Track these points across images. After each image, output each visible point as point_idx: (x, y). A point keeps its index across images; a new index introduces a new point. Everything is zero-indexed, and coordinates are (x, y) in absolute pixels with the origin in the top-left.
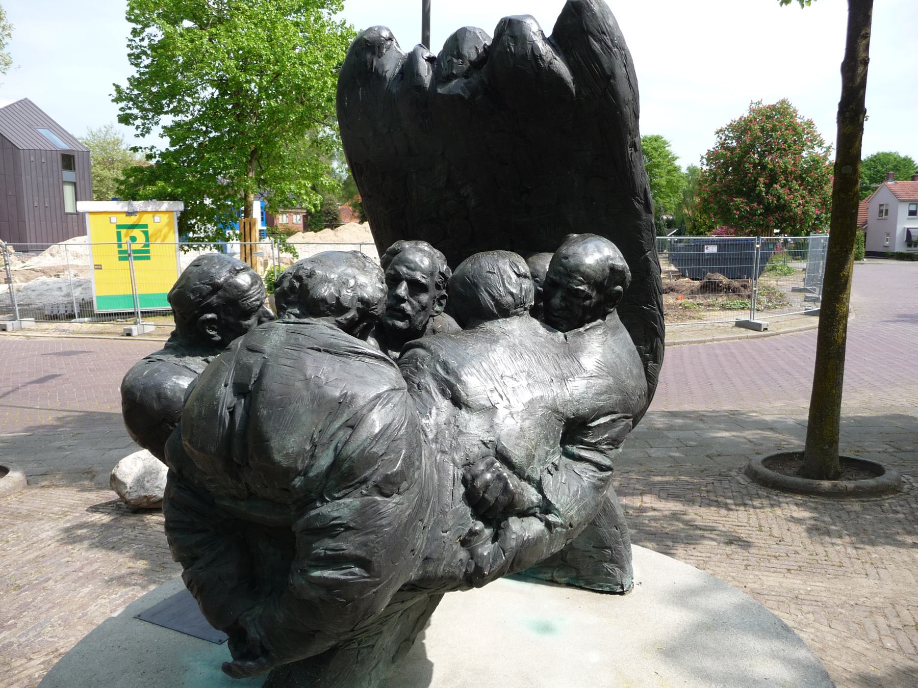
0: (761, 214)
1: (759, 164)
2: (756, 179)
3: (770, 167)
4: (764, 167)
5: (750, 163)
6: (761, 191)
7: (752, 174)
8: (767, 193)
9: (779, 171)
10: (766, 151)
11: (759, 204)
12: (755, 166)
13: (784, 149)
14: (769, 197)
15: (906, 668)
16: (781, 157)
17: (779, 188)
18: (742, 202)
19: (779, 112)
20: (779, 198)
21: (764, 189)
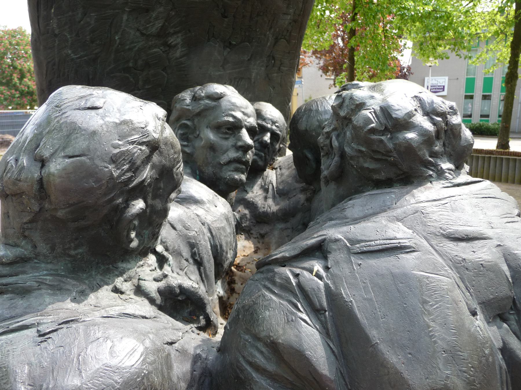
0: (18, 97)
1: (12, 65)
2: (11, 75)
3: (19, 67)
4: (15, 68)
5: (6, 65)
6: (16, 83)
7: (8, 71)
8: (20, 84)
9: (25, 70)
10: (15, 57)
11: (16, 90)
12: (9, 66)
13: (27, 58)
14: (22, 86)
15: (197, 205)
16: (25, 62)
17: (28, 81)
18: (5, 90)
19: (19, 34)
20: (28, 88)
21: (18, 82)
